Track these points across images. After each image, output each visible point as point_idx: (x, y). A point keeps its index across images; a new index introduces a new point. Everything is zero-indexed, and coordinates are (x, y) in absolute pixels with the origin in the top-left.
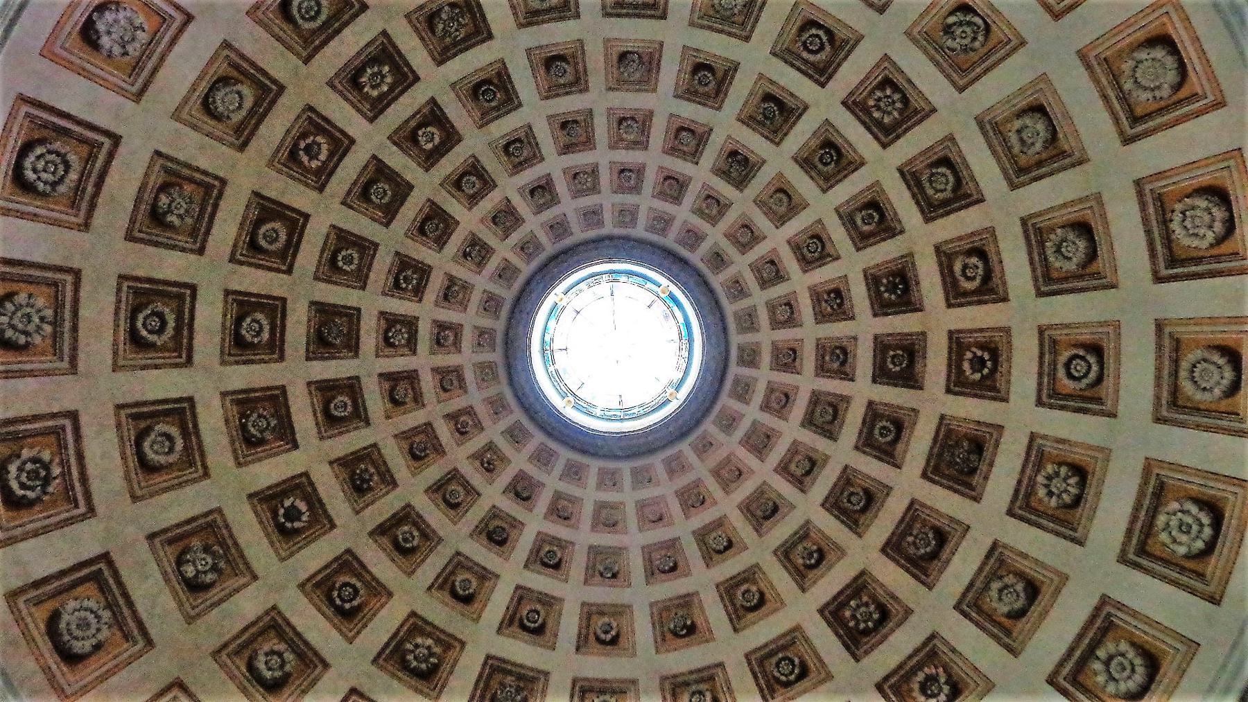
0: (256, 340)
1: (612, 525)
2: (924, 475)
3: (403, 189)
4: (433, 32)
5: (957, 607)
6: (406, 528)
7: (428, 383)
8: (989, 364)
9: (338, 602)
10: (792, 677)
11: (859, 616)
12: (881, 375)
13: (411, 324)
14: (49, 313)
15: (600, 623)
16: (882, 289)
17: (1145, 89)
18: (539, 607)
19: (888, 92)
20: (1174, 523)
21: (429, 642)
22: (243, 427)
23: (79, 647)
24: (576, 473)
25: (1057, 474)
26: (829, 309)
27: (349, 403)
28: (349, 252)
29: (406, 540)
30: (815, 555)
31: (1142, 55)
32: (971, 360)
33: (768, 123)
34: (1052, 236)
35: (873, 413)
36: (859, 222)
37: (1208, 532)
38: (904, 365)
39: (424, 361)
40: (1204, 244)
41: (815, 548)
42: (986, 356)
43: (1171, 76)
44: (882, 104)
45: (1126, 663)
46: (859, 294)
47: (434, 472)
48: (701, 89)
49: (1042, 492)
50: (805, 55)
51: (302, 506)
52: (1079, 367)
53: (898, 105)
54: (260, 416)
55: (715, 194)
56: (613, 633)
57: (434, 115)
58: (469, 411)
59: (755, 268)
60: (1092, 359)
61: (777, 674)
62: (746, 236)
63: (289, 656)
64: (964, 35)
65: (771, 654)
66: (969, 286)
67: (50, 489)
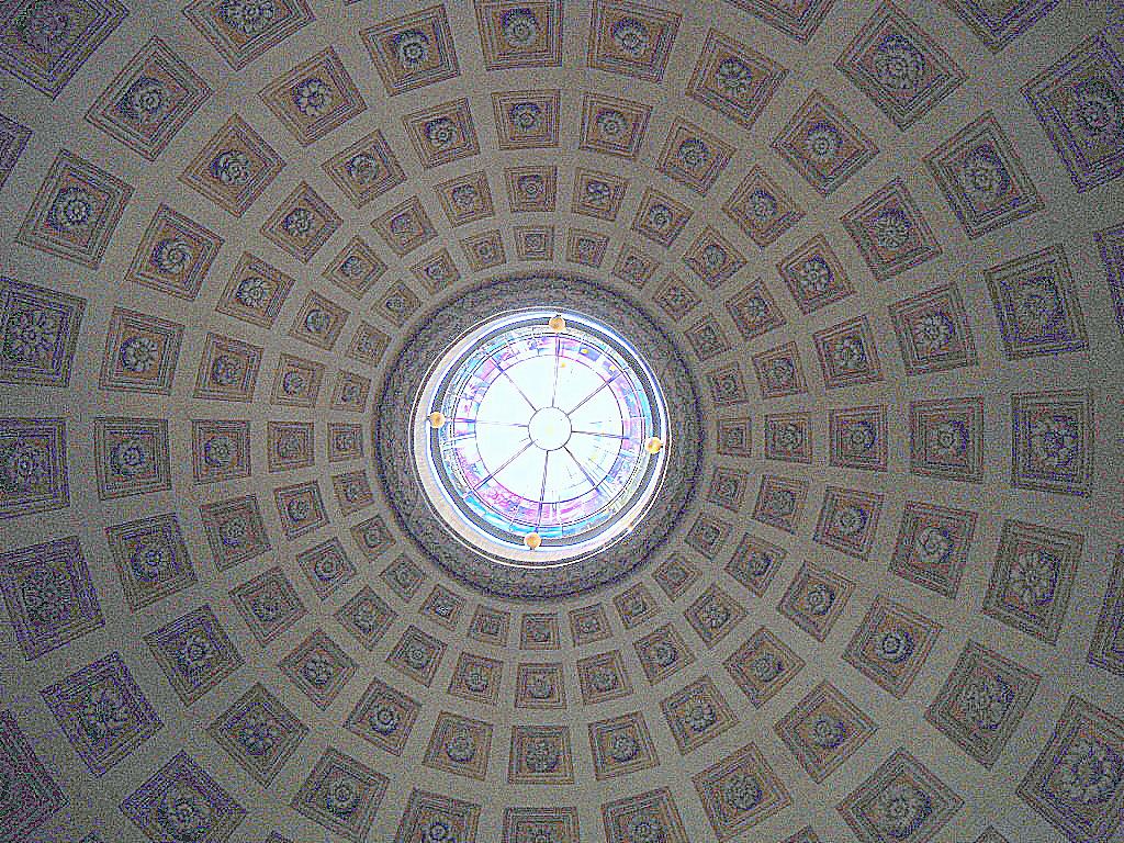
1: (396, 221)
7: (739, 241)
13: (809, 302)
15: (328, 100)
39: (762, 265)
41: (139, 368)
46: (295, 701)
47: (657, 139)
58: (667, 240)
59: (435, 647)
62: (474, 677)
65: (103, 210)
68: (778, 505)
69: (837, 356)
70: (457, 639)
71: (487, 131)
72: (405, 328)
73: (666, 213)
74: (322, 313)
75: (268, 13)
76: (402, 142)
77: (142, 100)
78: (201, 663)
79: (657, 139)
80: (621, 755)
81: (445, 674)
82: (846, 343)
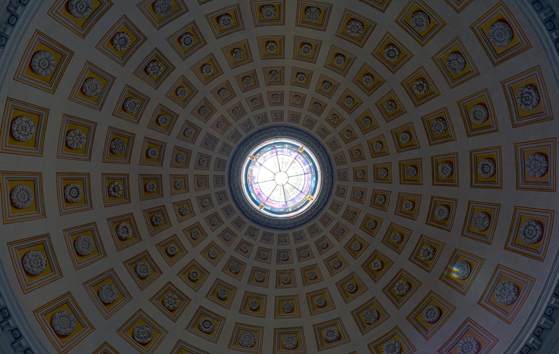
0: (444, 164)
2: (134, 135)
3: (386, 241)
4: (378, 312)
5: (115, 79)
6: (369, 85)
7: (367, 153)
8: (112, 190)
9: (395, 49)
10: (184, 37)
11: (157, 68)
12: (158, 178)
14: (527, 169)
15: (275, 50)
16: (162, 218)
17: (65, 316)
18: (304, 54)
19: (171, 306)
20: (28, 130)
21: (352, 35)
22: (446, 125)
23: (500, 25)
24: (294, 117)
25: (77, 144)
26: (185, 206)
27: (401, 140)
28: (407, 209)
29: (369, 79)
30: (179, 93)
31: (69, 330)
32: (119, 190)
33: (223, 288)
34: (93, 250)
35: (160, 161)
36: (176, 247)
37: (15, 128)
38: (148, 184)
39: (369, 162)
40: (31, 252)
41: (180, 96)
42: (113, 193)
43: (55, 322)
44: (173, 301)
45: (42, 66)
46: (172, 215)
48: (254, 300)
49: (83, 135)
50: (210, 319)
51: (416, 91)
52: (74, 193)
53: (166, 301)
54: (439, 131)
55: (243, 253)
56: (268, 46)
57: (374, 275)
60: (69, 198)
61: (192, 37)
62: (227, 236)
63: (414, 25)
64: (143, 333)
66: (124, 224)
67: (520, 93)
68: (339, 232)
69: (377, 199)
70: (228, 223)
71: (314, 84)
72: (261, 126)
73: (351, 134)
74: (239, 110)
75: (273, 16)
76: (288, 74)
77: (224, 20)
78: (151, 190)
79: (359, 112)
80: (258, 279)
81: (219, 230)
82: (382, 196)
